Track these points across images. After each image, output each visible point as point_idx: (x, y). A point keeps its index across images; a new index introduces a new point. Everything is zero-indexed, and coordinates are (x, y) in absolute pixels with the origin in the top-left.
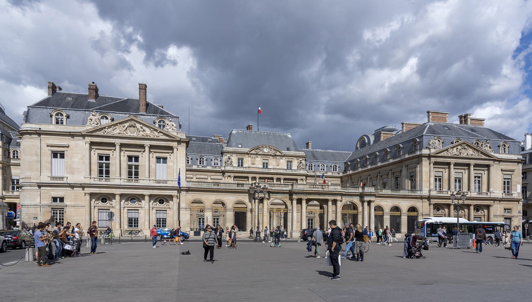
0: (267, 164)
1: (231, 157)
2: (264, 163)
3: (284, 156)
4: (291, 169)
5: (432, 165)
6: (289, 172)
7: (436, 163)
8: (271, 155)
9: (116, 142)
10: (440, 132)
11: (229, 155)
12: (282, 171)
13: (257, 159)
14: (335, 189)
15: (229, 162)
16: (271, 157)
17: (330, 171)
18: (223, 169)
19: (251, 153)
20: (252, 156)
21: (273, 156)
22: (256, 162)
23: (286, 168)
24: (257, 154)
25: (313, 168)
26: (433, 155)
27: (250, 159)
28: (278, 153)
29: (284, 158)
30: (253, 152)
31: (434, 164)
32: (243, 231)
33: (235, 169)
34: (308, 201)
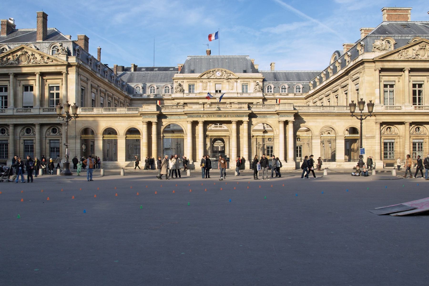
1: (182, 84)
4: (247, 92)
5: (377, 72)
6: (245, 95)
7: (383, 70)
8: (224, 78)
9: (10, 72)
10: (393, 31)
11: (180, 81)
12: (235, 95)
13: (209, 83)
14: (241, 108)
15: (178, 89)
16: (225, 81)
17: (293, 92)
18: (174, 96)
20: (204, 80)
22: (208, 87)
23: (241, 91)
24: (208, 78)
25: (272, 90)
26: (377, 59)
27: (201, 84)
28: (232, 77)
30: (205, 77)
31: (380, 71)
32: (126, 159)
33: (185, 96)
34: (206, 123)
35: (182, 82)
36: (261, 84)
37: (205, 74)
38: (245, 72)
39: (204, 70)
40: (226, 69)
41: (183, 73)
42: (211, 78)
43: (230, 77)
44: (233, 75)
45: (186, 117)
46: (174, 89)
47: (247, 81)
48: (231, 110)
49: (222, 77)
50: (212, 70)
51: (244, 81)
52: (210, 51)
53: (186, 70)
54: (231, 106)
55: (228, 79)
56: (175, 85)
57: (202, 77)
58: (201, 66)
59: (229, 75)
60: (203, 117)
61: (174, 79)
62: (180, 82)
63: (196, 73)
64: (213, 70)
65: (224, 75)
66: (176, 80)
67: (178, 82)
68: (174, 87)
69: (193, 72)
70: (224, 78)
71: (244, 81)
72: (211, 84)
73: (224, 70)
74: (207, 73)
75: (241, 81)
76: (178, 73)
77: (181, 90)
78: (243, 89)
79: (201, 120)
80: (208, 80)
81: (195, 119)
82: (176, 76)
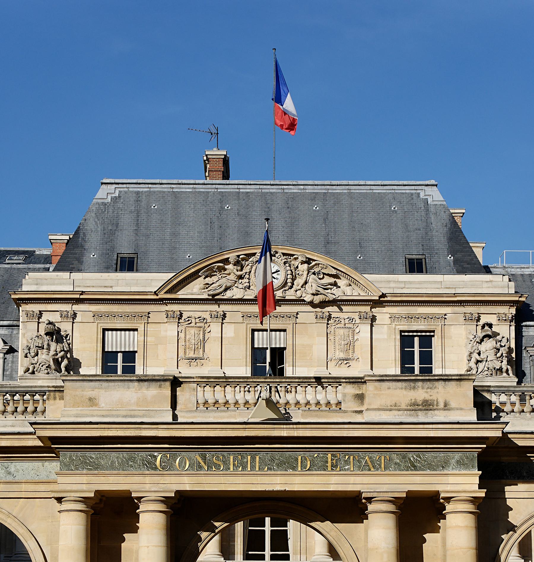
0: (278, 354)
1: (65, 327)
2: (257, 354)
3: (380, 302)
8: (300, 301)
13: (215, 328)
15: (43, 356)
16: (307, 314)
19: (182, 294)
20: (188, 310)
21: (311, 304)
22: (212, 349)
24: (214, 300)
27: (171, 330)
28: (344, 290)
29: (383, 314)
35: (64, 316)
36: (506, 332)
37: (195, 276)
38: (415, 266)
39: (190, 256)
40: (314, 250)
41: (71, 270)
42: (228, 294)
43: (336, 293)
44: (352, 282)
45: (49, 468)
46: (20, 354)
47: (427, 317)
48: (359, 418)
49: (290, 295)
50: (232, 256)
51: (410, 317)
52: (226, 161)
53: (92, 256)
54: (360, 397)
55: (323, 304)
56: (27, 334)
57: (182, 294)
58: (175, 234)
59: (328, 280)
60: (167, 466)
61: (20, 302)
62: (55, 318)
63: (146, 271)
64: (242, 253)
65: (299, 281)
66: (36, 308)
67: (45, 318)
68: (21, 344)
69: (128, 264)
70: (300, 301)
71: (410, 317)
72: (229, 330)
73: (301, 254)
74: (210, 272)
75: (392, 317)
76: (47, 270)
77: (58, 363)
78: (406, 358)
79: (153, 486)
80: (215, 308)
81: (113, 482)
82: (34, 282)
